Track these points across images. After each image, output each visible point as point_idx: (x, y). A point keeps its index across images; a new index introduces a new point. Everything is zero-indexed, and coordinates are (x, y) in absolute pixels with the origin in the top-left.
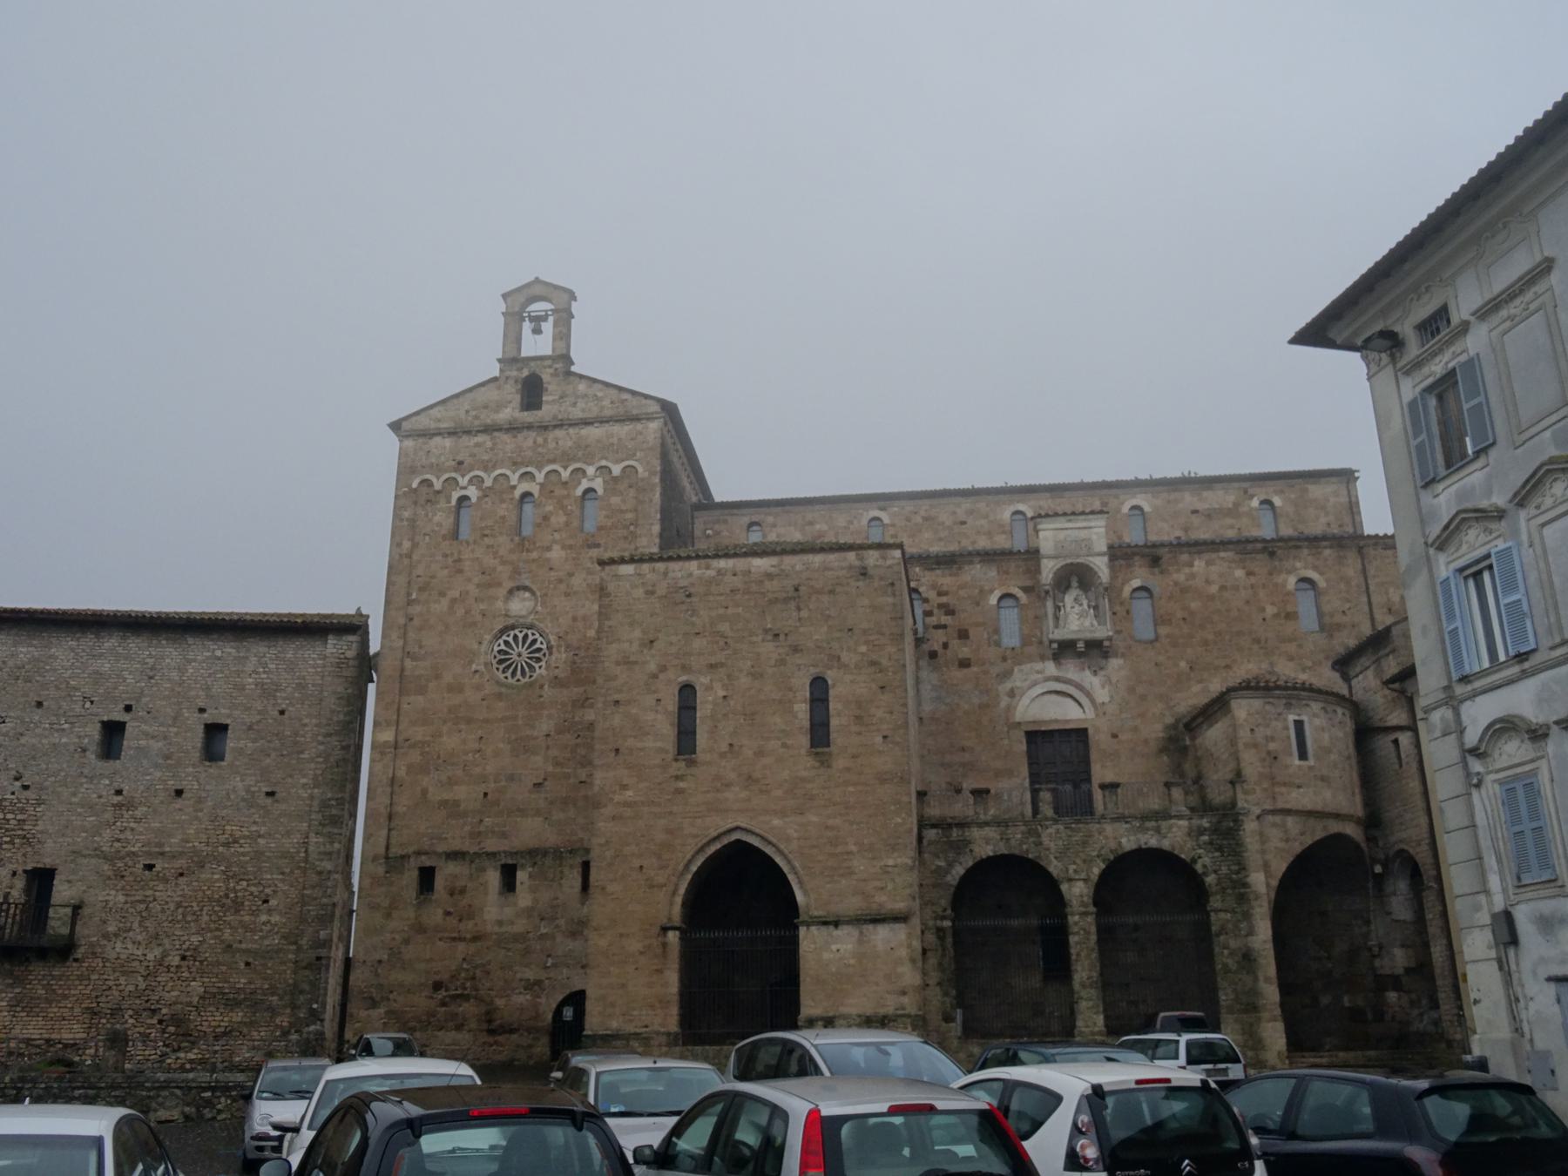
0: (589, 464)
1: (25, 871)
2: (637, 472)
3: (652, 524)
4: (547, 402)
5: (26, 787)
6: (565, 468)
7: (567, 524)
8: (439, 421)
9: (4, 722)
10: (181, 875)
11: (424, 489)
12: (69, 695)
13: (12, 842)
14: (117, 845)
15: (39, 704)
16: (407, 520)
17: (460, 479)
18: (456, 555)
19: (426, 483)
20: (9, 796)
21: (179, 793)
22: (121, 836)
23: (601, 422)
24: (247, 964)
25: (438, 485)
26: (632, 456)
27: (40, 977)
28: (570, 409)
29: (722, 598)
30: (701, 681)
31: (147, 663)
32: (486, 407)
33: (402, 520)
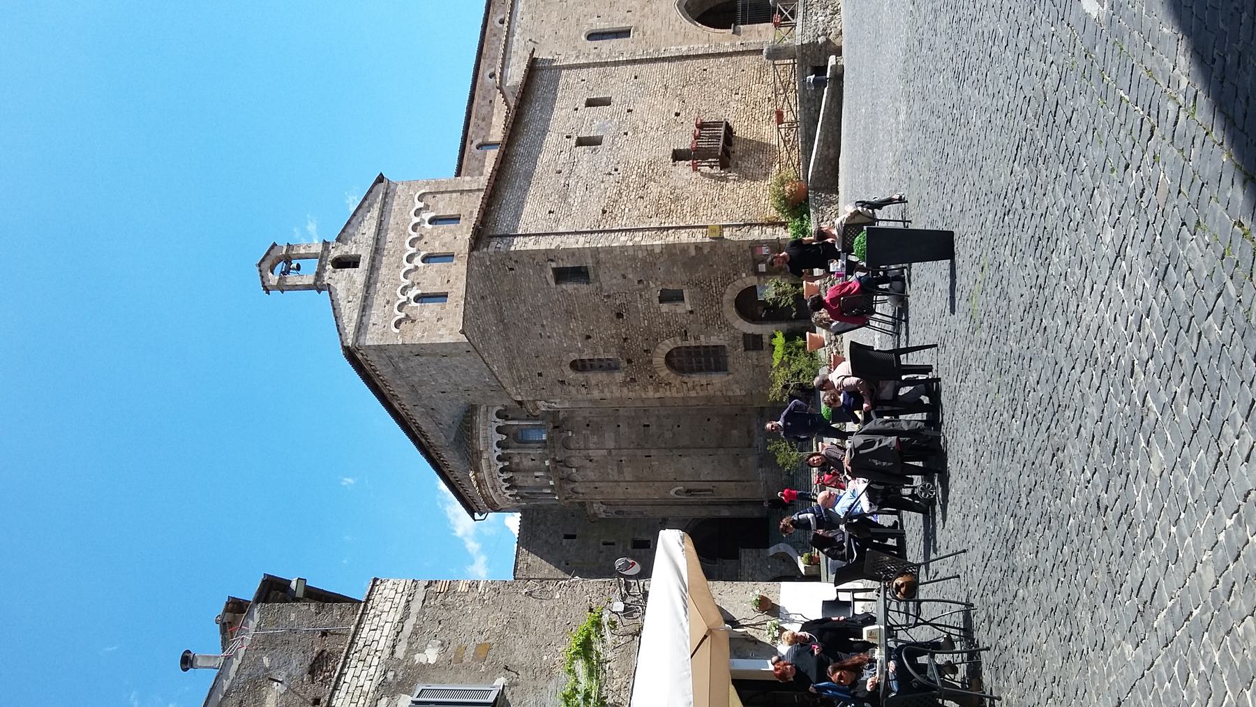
0: (411, 221)
1: (674, 161)
2: (424, 194)
3: (464, 181)
4: (357, 251)
5: (616, 170)
6: (410, 235)
7: (451, 231)
8: (351, 320)
9: (568, 185)
10: (684, 102)
11: (403, 325)
12: (555, 160)
13: (653, 170)
14: (660, 129)
15: (560, 172)
16: (424, 332)
17: (400, 301)
18: (457, 299)
19: (397, 324)
20: (621, 175)
21: (629, 111)
22: (655, 128)
23: (382, 216)
24: (743, 70)
25: (402, 315)
26: (412, 197)
27: (745, 145)
28: (366, 236)
29: (535, 23)
30: (586, 29)
31: (539, 134)
32: (349, 289)
33: (423, 336)
